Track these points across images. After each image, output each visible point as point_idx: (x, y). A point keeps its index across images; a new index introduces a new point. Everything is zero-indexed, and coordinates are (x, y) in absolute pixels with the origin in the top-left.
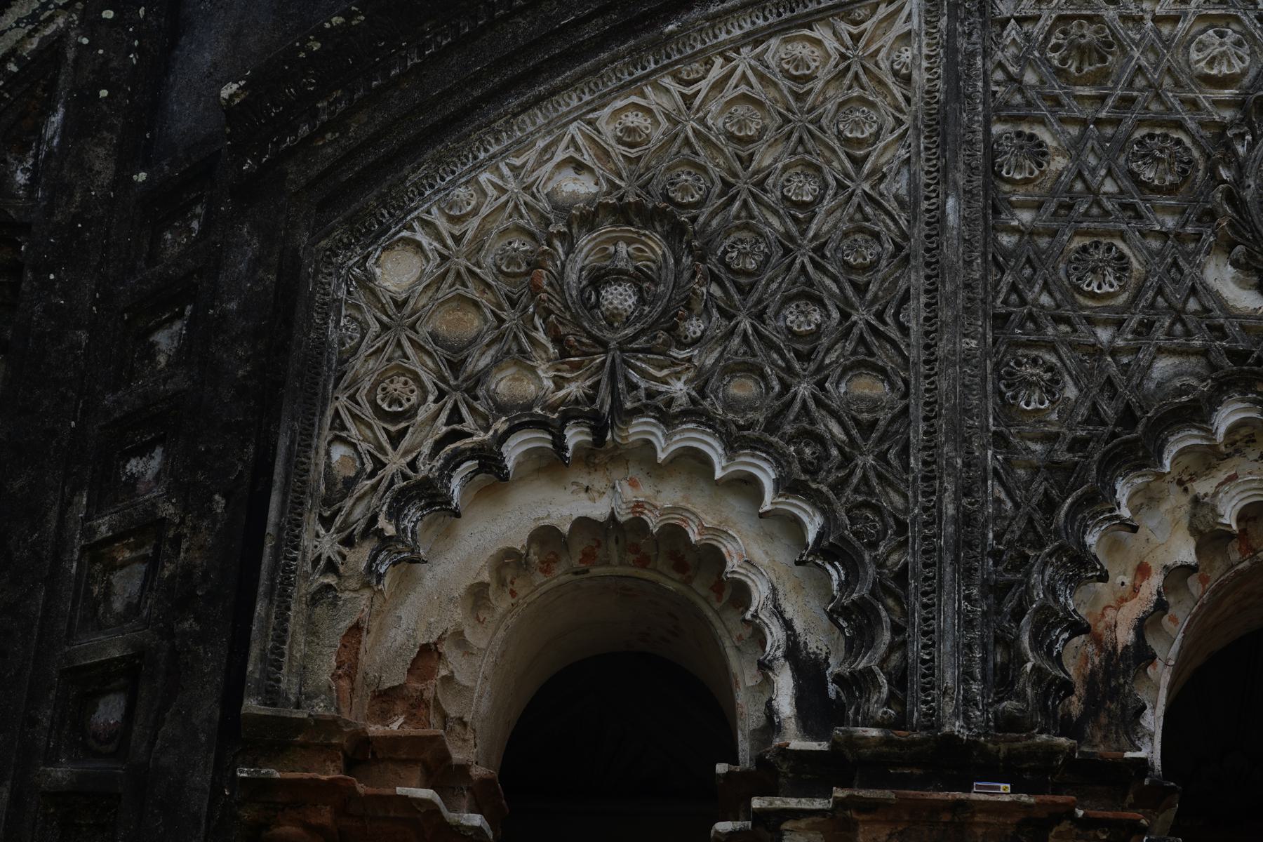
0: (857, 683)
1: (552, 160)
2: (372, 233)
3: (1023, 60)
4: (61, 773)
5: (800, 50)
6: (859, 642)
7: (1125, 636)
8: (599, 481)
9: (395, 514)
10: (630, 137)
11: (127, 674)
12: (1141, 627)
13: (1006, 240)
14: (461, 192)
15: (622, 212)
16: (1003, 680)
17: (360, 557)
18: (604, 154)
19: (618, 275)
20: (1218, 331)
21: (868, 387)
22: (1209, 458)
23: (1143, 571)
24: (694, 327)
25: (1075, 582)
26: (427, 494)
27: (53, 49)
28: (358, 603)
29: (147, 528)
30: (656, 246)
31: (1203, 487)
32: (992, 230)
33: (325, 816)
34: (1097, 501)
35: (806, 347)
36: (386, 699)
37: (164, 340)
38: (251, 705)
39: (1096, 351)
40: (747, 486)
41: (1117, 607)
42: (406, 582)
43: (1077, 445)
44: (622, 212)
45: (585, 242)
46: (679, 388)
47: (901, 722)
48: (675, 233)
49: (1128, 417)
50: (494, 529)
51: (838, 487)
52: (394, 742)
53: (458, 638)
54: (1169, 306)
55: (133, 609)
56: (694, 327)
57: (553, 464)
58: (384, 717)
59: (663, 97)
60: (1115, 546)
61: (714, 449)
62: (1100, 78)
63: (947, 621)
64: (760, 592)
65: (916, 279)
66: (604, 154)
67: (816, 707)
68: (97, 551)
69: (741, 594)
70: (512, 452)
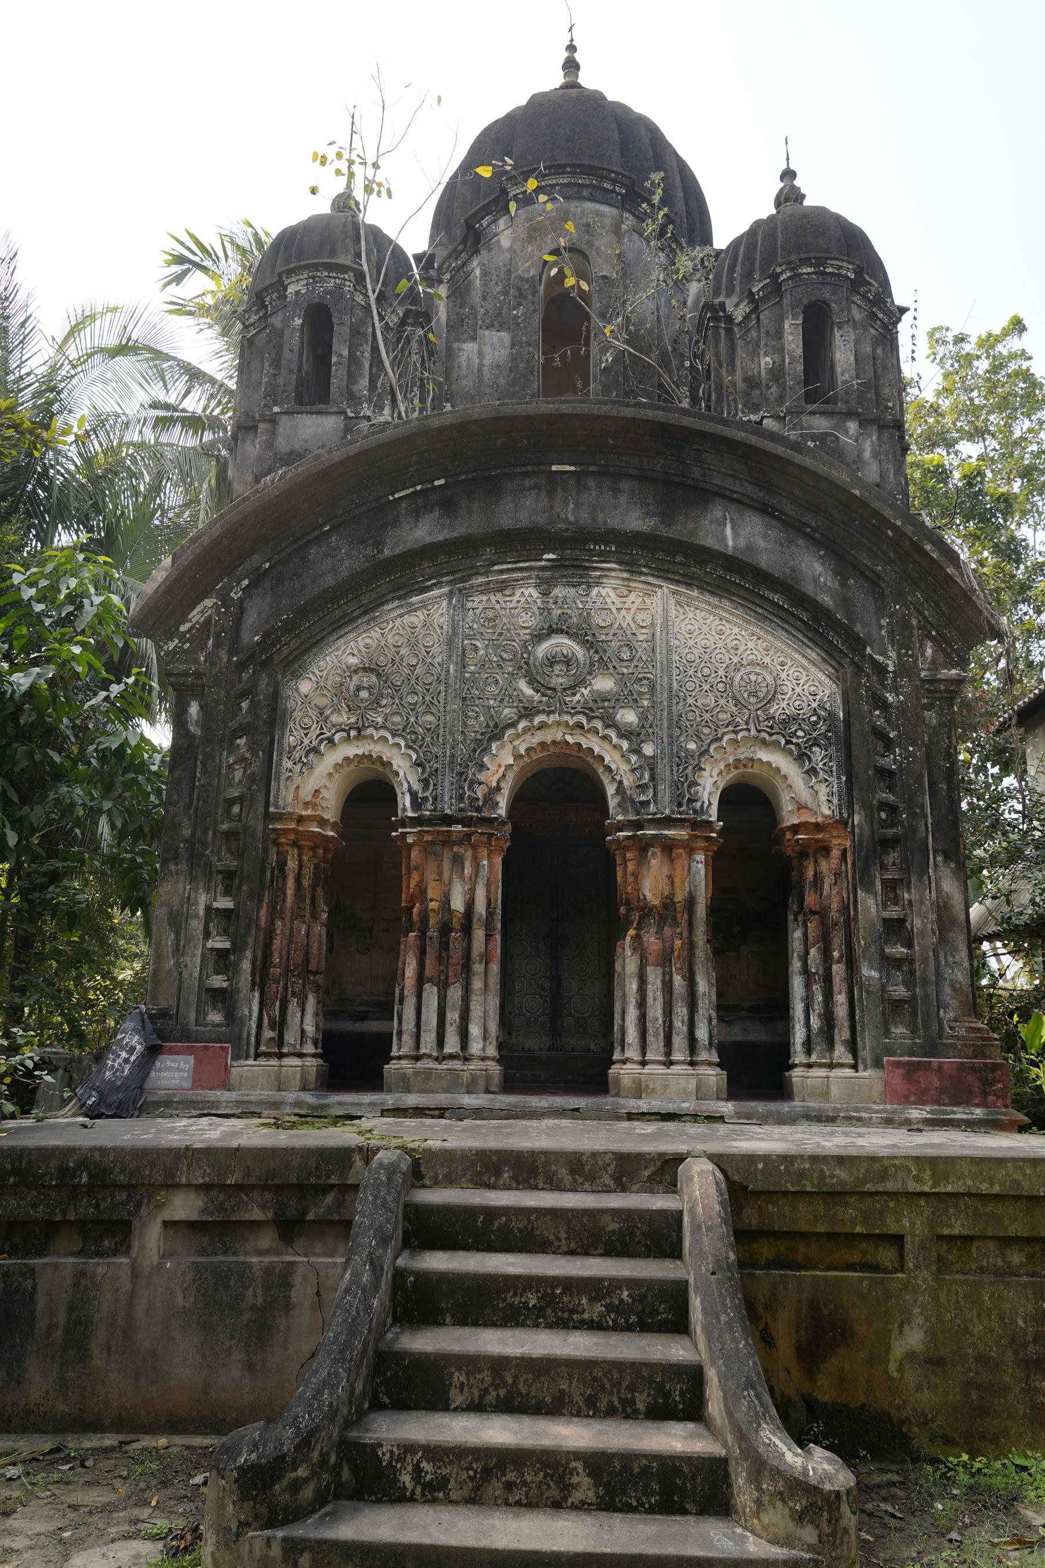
0: (425, 799)
1: (344, 654)
2: (297, 675)
3: (473, 621)
4: (225, 827)
5: (413, 619)
6: (425, 788)
7: (494, 784)
8: (360, 744)
9: (306, 756)
10: (367, 646)
11: (241, 799)
12: (498, 782)
13: (467, 675)
14: (322, 663)
15: (365, 669)
16: (461, 798)
17: (298, 767)
18: (360, 651)
19: (364, 688)
20: (521, 701)
21: (429, 718)
22: (518, 736)
23: (500, 766)
24: (384, 702)
25: (480, 771)
26: (316, 750)
27: (209, 620)
28: (298, 780)
29: (243, 760)
30: (374, 679)
31: (516, 743)
32: (462, 673)
33: (292, 836)
34: (486, 750)
35: (413, 707)
36: (307, 804)
37: (244, 705)
38: (272, 809)
39: (489, 708)
40: (398, 745)
41: (491, 776)
42: (310, 774)
43: (483, 734)
44: (365, 669)
45: (355, 678)
46: (380, 720)
47: (435, 810)
48: (379, 675)
49: (496, 726)
50: (333, 757)
51: (420, 747)
52: (309, 816)
53: (325, 787)
54: (508, 695)
55: (240, 781)
56: (384, 702)
57: (348, 739)
58: (306, 809)
59: (376, 633)
60: (492, 760)
61: (389, 736)
62: (493, 627)
63: (447, 783)
64: (401, 774)
65: (442, 688)
66: (360, 651)
67: (417, 804)
68: (230, 766)
69: (397, 774)
70: (337, 738)
